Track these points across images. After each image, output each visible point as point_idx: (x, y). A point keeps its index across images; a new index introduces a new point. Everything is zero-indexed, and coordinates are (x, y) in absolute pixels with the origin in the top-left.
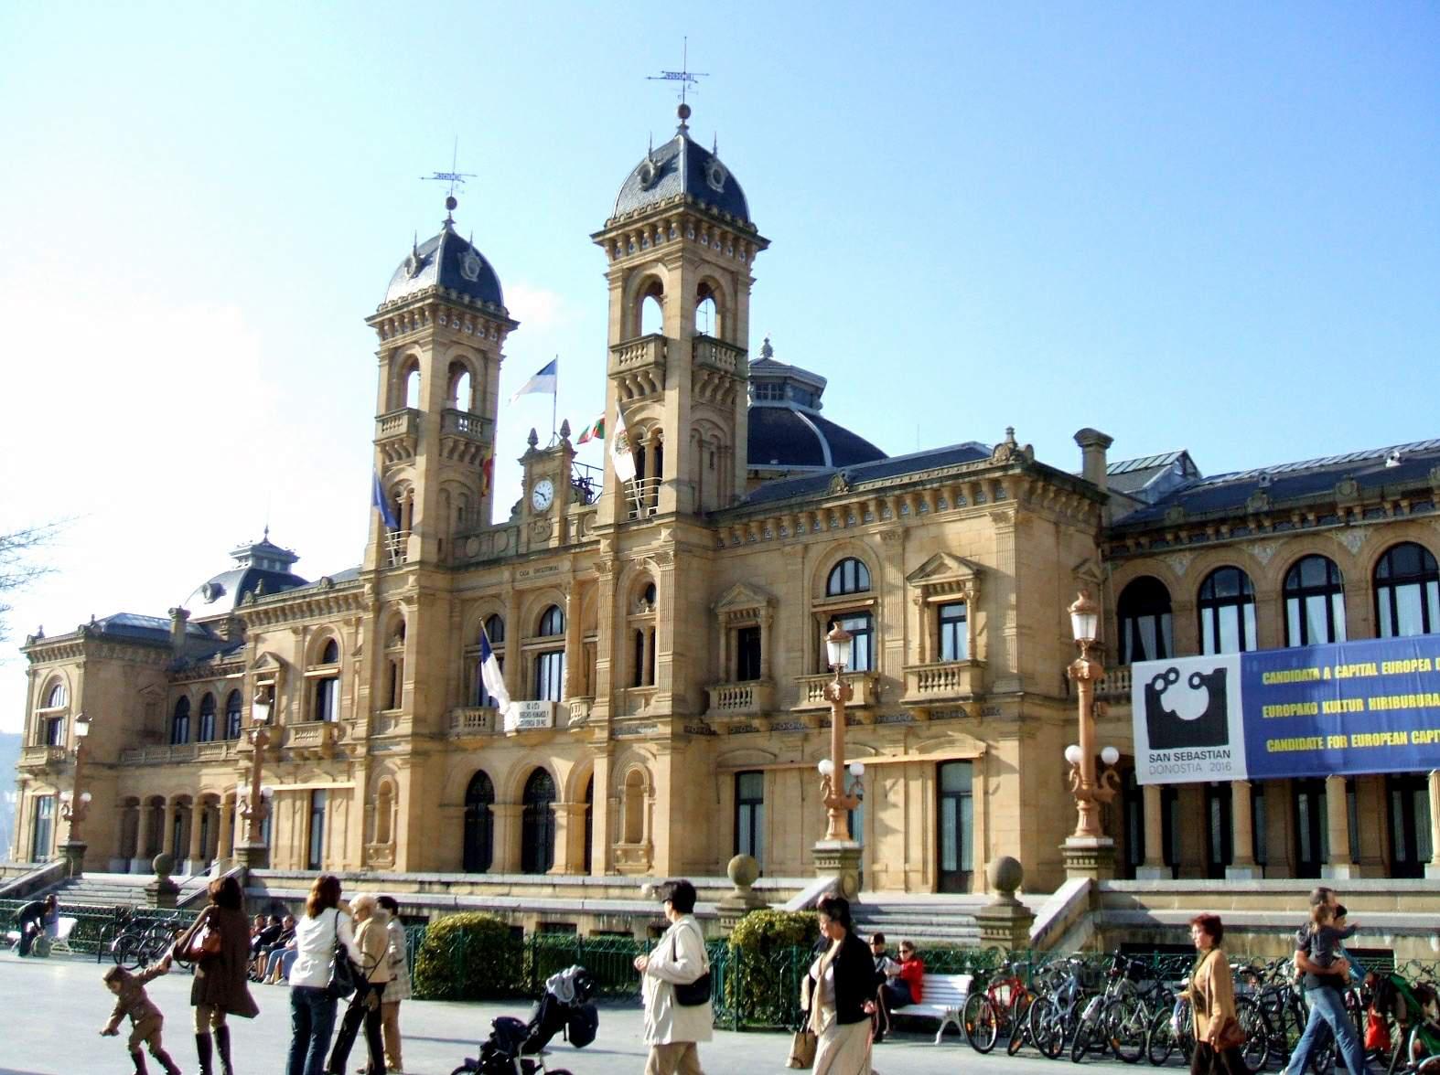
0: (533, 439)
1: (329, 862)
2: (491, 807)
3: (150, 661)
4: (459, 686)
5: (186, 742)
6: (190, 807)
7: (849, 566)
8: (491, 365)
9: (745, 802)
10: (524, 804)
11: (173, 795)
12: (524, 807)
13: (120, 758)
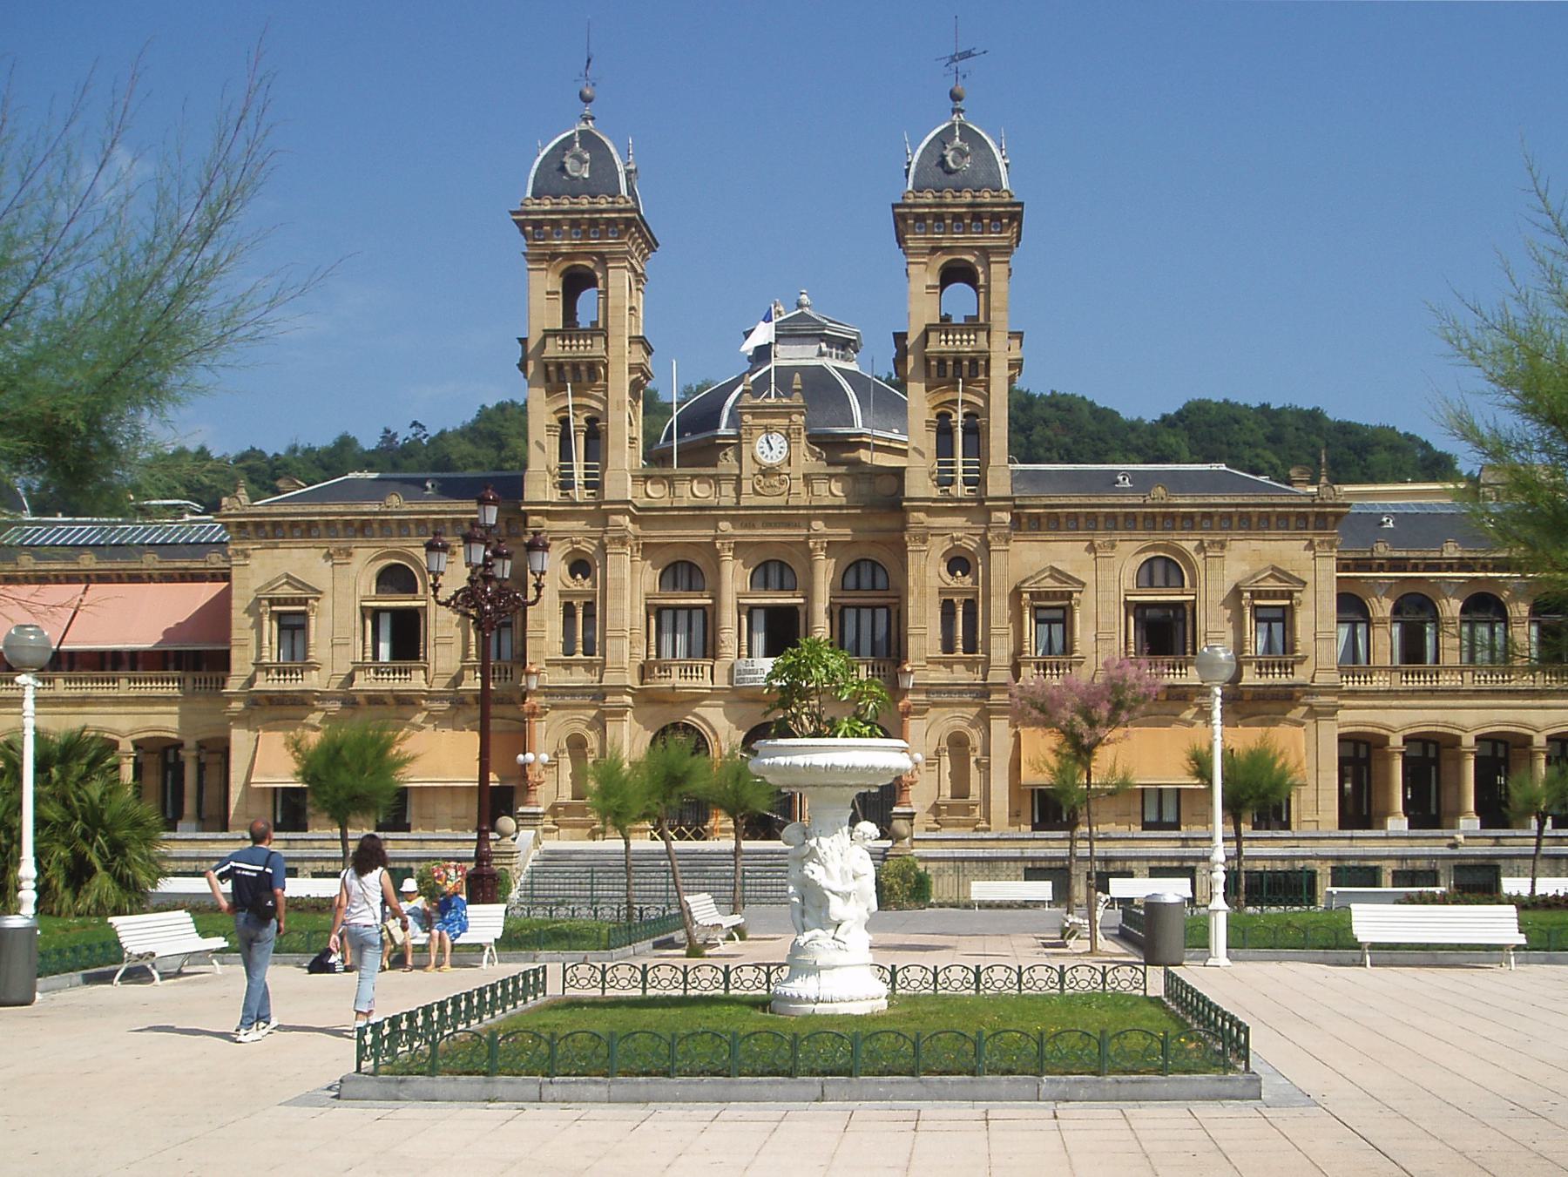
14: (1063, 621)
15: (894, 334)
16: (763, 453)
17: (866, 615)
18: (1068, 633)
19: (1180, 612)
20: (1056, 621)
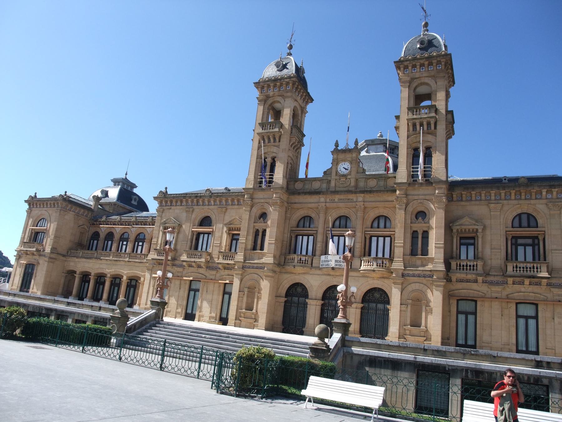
0: (337, 145)
1: (201, 314)
2: (307, 300)
3: (85, 215)
4: (287, 244)
5: (96, 249)
6: (75, 275)
7: (524, 218)
8: (304, 114)
9: (462, 313)
10: (285, 297)
11: (96, 272)
12: (286, 299)
13: (68, 252)
14: (473, 244)
15: (395, 116)
16: (340, 170)
17: (381, 239)
18: (476, 250)
19: (536, 241)
20: (471, 244)
